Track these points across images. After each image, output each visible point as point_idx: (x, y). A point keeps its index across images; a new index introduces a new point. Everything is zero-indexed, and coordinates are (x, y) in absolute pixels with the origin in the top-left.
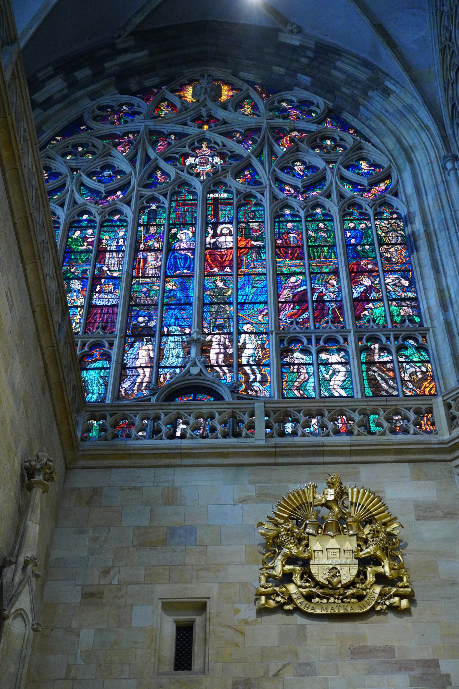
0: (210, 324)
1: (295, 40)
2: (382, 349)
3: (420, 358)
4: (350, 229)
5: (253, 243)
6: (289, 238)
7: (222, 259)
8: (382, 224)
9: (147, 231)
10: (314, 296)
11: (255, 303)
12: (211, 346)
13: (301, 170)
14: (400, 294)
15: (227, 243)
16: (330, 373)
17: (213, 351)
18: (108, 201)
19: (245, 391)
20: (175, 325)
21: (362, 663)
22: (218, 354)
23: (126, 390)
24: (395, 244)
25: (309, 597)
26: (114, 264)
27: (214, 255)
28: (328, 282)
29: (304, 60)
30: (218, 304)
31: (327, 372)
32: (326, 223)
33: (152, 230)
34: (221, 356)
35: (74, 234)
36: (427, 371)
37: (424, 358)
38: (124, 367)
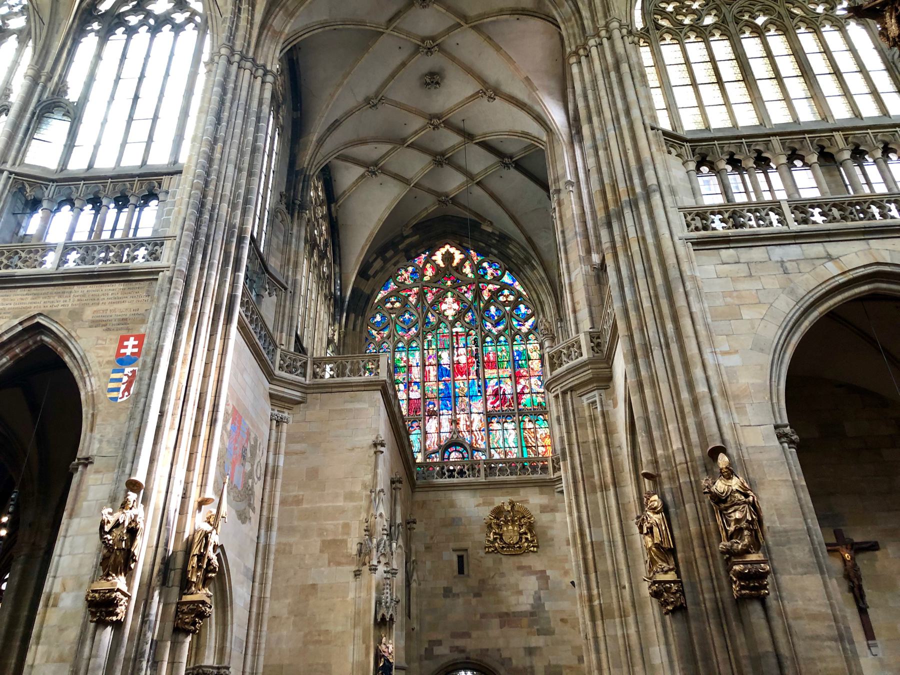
1: (490, 230)
2: (530, 421)
21: (521, 572)
25: (503, 547)
29: (494, 241)
33: (431, 352)
38: (426, 433)
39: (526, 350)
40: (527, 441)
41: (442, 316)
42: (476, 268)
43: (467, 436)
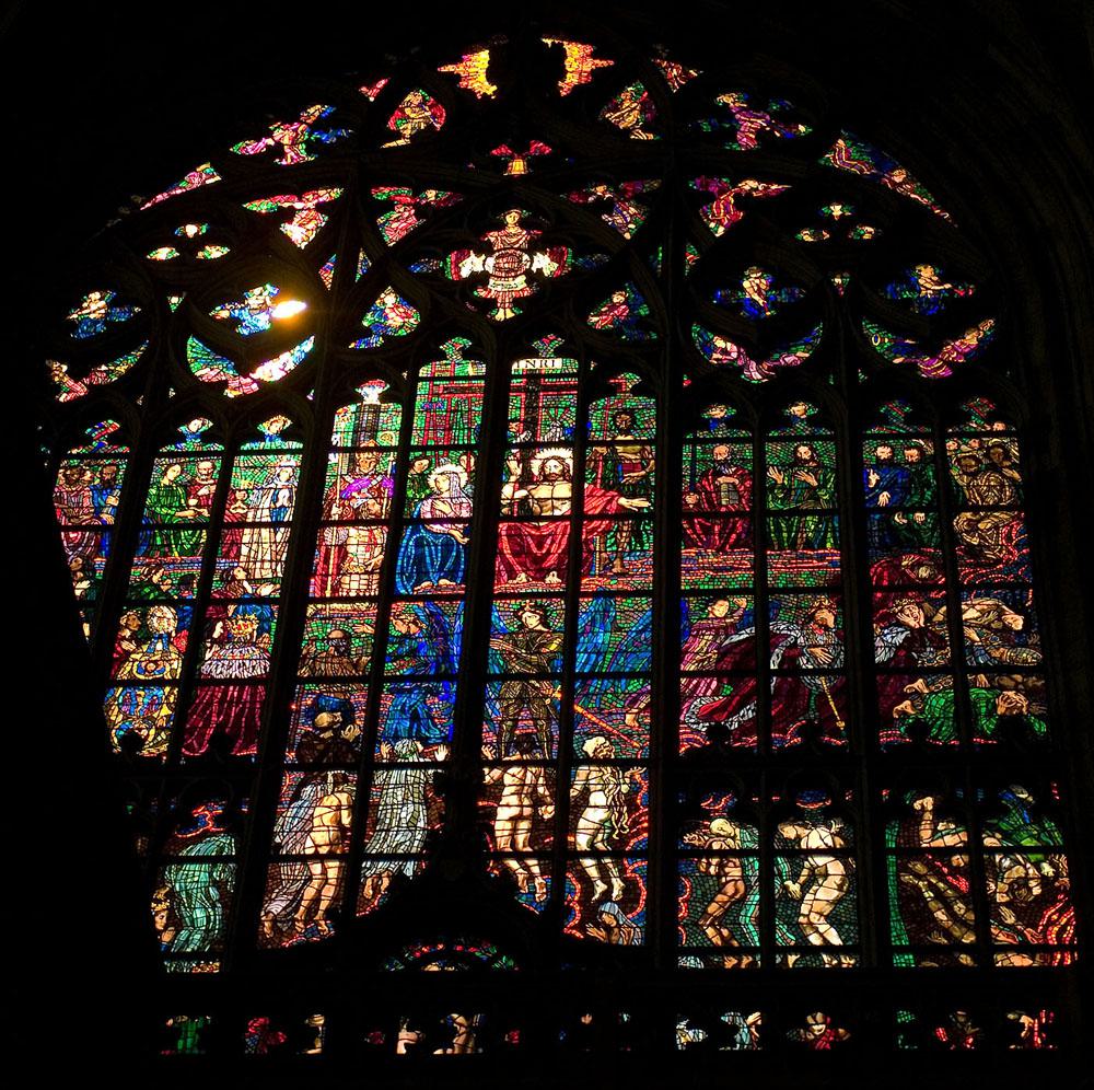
0: (499, 736)
2: (939, 814)
3: (1038, 839)
4: (880, 465)
5: (623, 501)
6: (718, 489)
7: (540, 547)
8: (964, 447)
10: (774, 658)
11: (617, 676)
12: (498, 798)
13: (759, 292)
14: (997, 654)
15: (556, 503)
16: (802, 879)
17: (503, 813)
19: (581, 927)
20: (410, 737)
22: (515, 820)
23: (274, 921)
24: (996, 508)
27: (520, 536)
28: (812, 618)
31: (795, 877)
32: (818, 444)
34: (524, 825)
35: (164, 473)
37: (1051, 837)
39: (941, 460)
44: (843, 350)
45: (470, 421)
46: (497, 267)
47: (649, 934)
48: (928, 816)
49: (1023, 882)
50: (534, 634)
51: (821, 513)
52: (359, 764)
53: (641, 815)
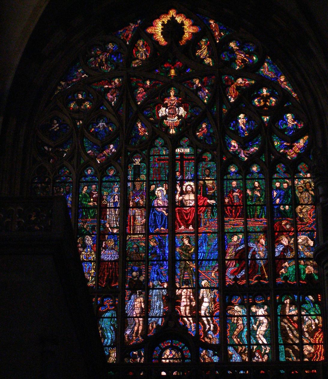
0: (180, 279)
2: (291, 304)
3: (315, 312)
4: (277, 189)
6: (233, 196)
7: (187, 217)
8: (299, 183)
9: (134, 186)
10: (249, 255)
11: (209, 260)
12: (181, 299)
13: (243, 124)
14: (306, 254)
16: (257, 324)
18: (105, 155)
20: (157, 280)
22: (185, 306)
23: (128, 336)
24: (307, 204)
26: (113, 221)
27: (182, 213)
28: (259, 242)
30: (185, 260)
31: (255, 323)
34: (188, 308)
35: (83, 189)
36: (319, 324)
37: (318, 312)
39: (293, 187)
40: (286, 336)
41: (158, 127)
42: (217, 50)
43: (189, 322)
44: (267, 148)
45: (165, 172)
46: (169, 113)
47: (220, 340)
48: (288, 305)
49: (310, 325)
50: (187, 247)
51: (261, 206)
52: (143, 288)
53: (217, 305)
